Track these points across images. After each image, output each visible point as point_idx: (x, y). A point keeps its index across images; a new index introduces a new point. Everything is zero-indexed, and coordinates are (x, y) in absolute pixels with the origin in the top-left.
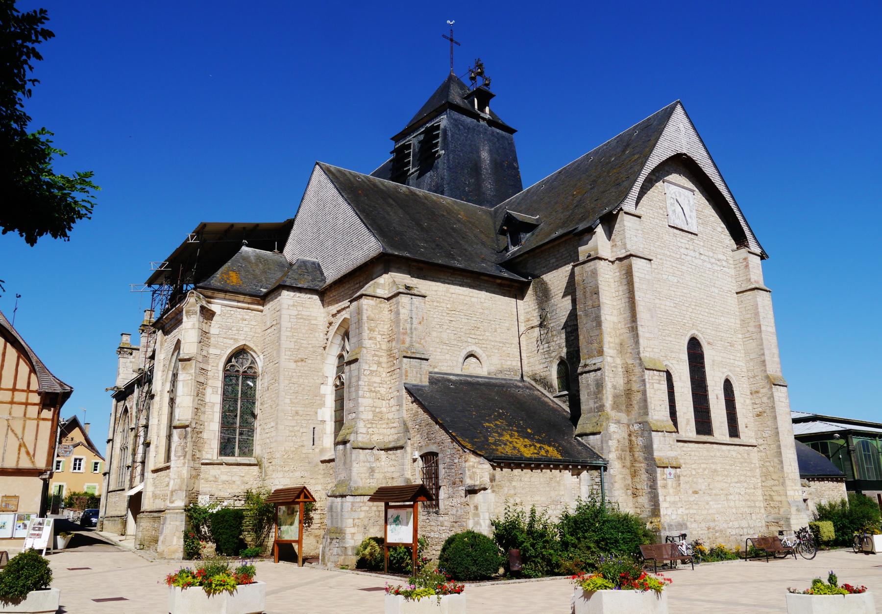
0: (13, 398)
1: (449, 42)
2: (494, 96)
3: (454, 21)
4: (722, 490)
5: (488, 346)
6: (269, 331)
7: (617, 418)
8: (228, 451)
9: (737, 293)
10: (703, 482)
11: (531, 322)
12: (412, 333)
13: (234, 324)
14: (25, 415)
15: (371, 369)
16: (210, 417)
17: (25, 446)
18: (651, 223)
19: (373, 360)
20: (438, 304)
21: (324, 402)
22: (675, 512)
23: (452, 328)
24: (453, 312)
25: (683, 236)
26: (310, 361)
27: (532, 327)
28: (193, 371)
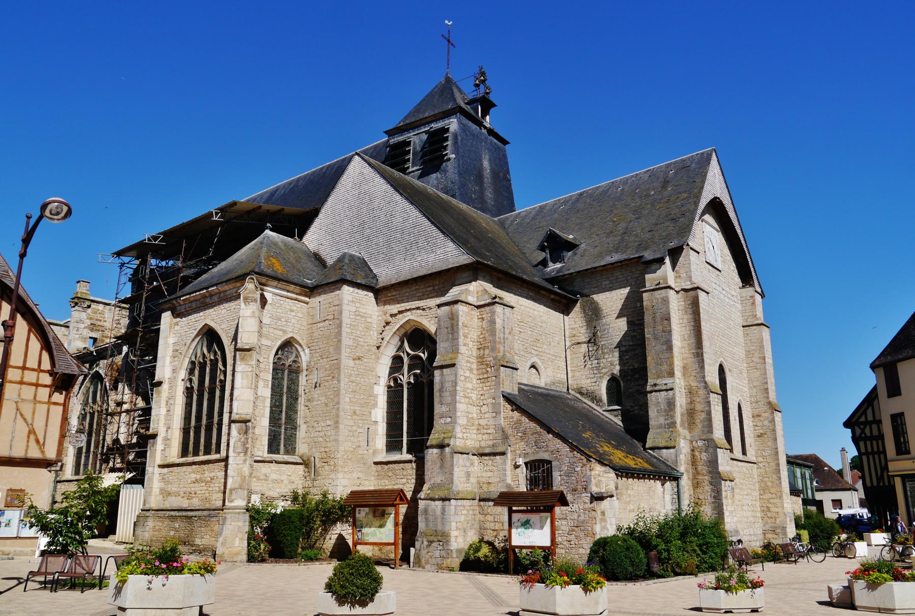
0: (22, 378)
1: (446, 42)
2: (496, 106)
3: (451, 22)
5: (546, 359)
6: (320, 325)
8: (274, 448)
9: (743, 327)
11: (577, 338)
12: (504, 343)
13: (283, 315)
15: (465, 375)
16: (262, 411)
17: (35, 433)
19: (467, 366)
21: (377, 402)
23: (521, 339)
24: (522, 324)
26: (365, 360)
27: (579, 343)
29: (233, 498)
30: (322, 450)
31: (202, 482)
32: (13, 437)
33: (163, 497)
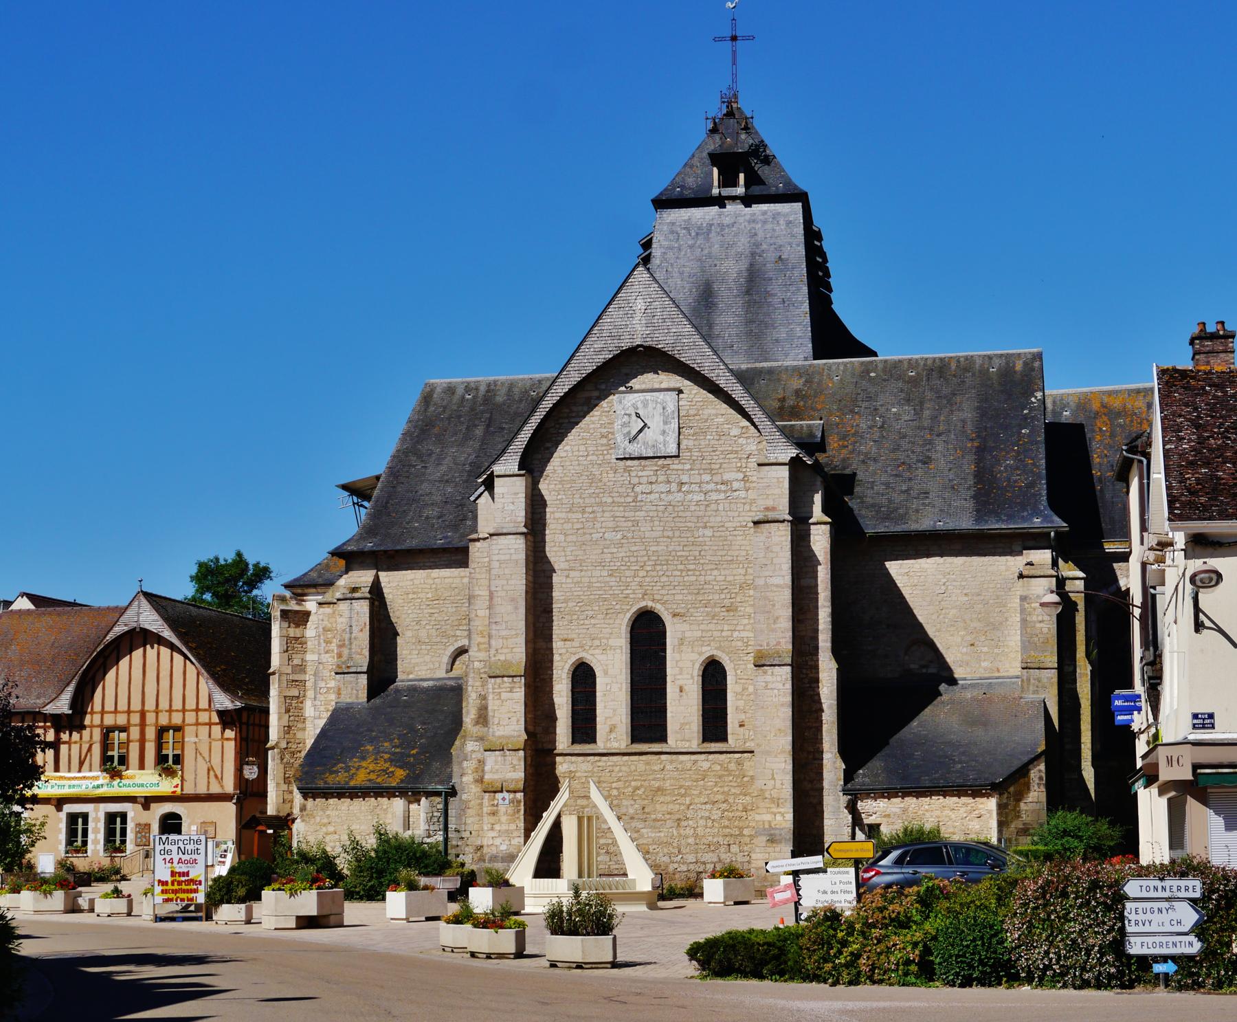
0: (197, 719)
4: (670, 813)
7: (480, 734)
10: (632, 805)
12: (351, 644)
14: (210, 736)
15: (328, 686)
17: (213, 769)
18: (579, 465)
20: (415, 596)
22: (507, 842)
24: (435, 602)
25: (644, 466)
28: (277, 686)
32: (196, 775)
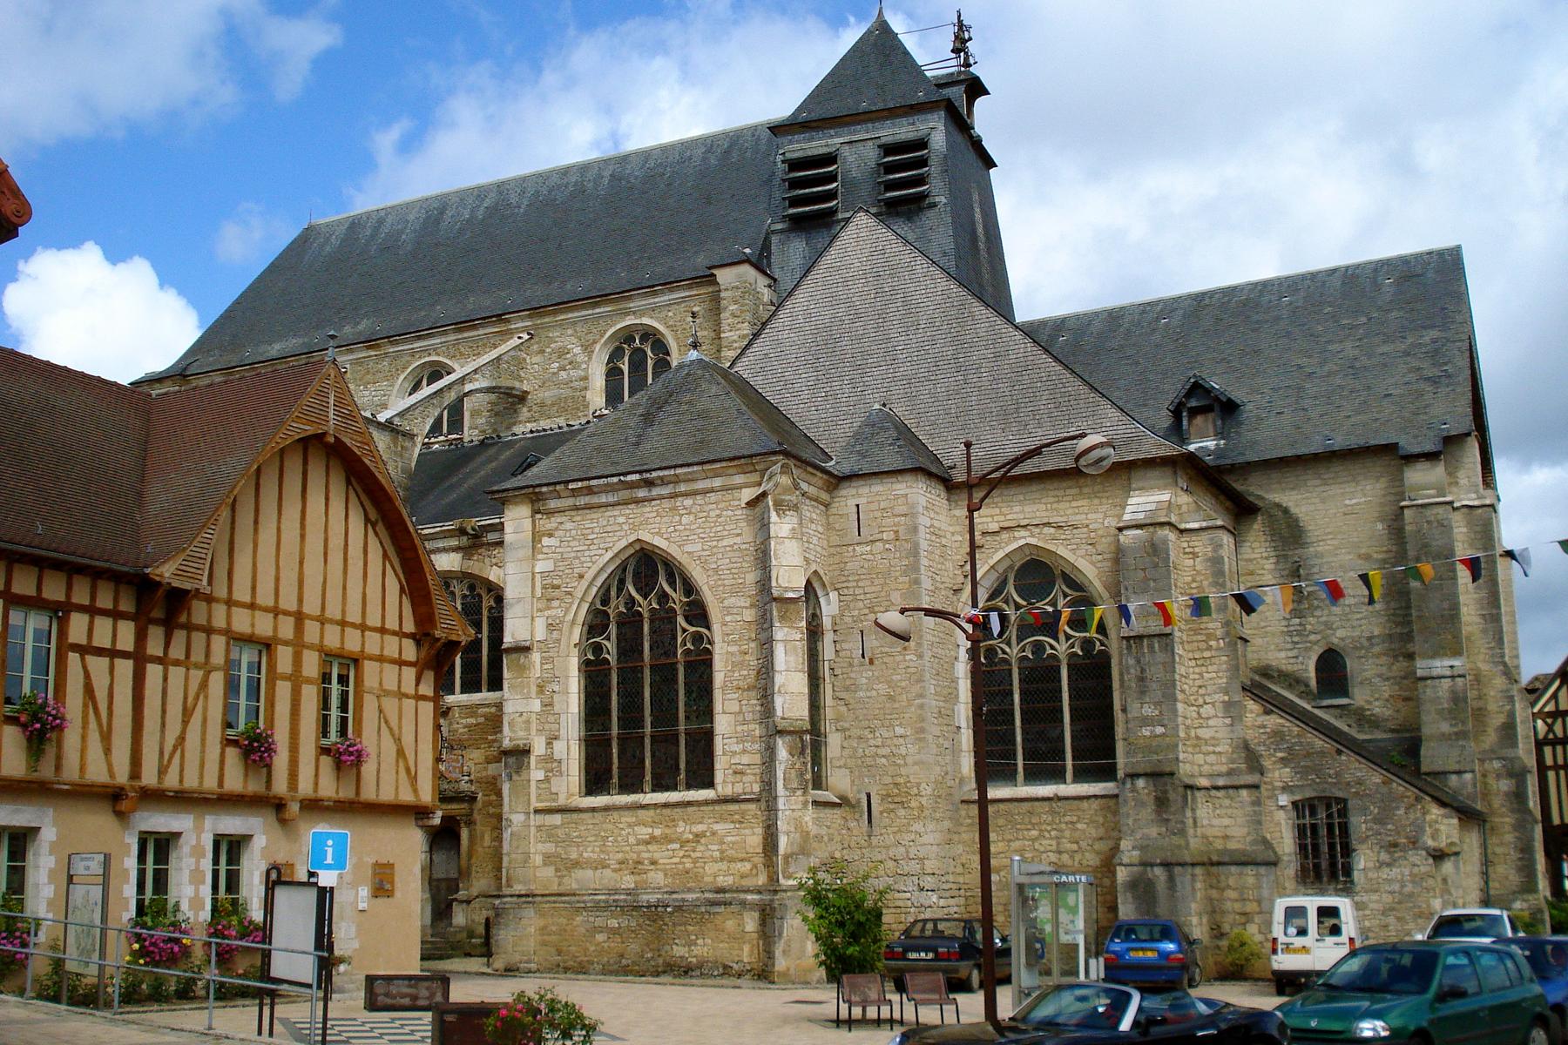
2: (989, 94)
11: (1258, 578)
28: (804, 624)
29: (791, 870)
30: (888, 780)
31: (671, 841)
33: (557, 870)
